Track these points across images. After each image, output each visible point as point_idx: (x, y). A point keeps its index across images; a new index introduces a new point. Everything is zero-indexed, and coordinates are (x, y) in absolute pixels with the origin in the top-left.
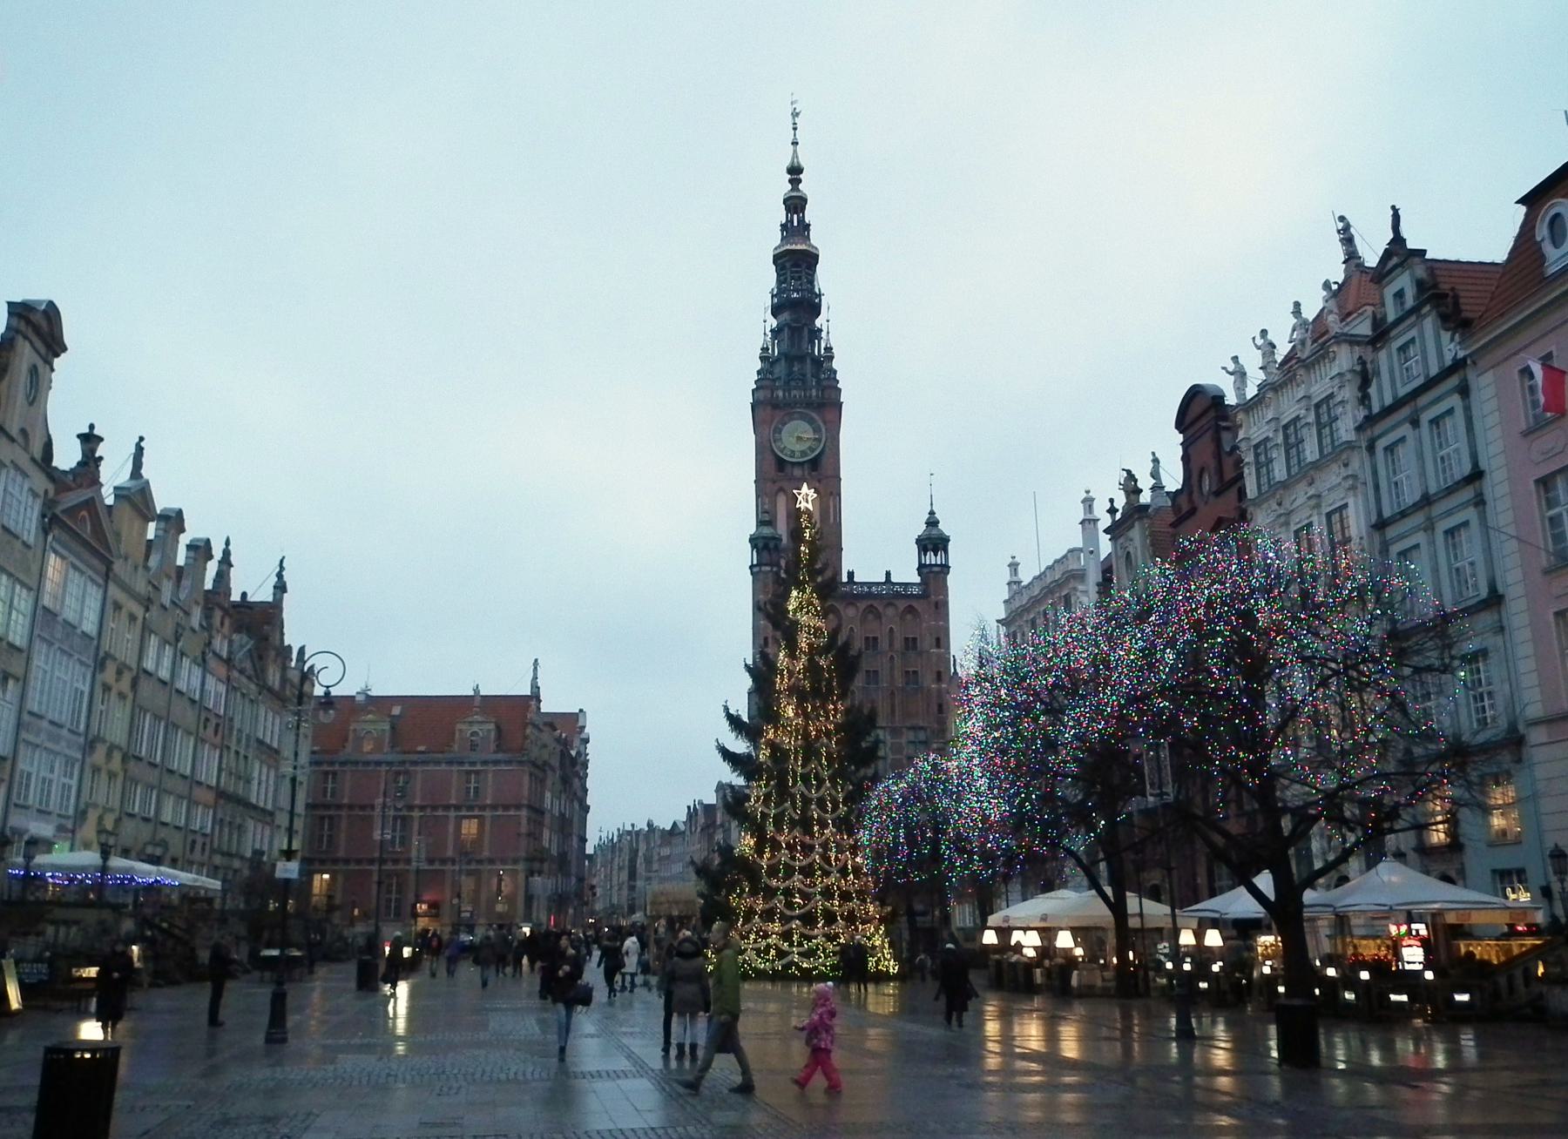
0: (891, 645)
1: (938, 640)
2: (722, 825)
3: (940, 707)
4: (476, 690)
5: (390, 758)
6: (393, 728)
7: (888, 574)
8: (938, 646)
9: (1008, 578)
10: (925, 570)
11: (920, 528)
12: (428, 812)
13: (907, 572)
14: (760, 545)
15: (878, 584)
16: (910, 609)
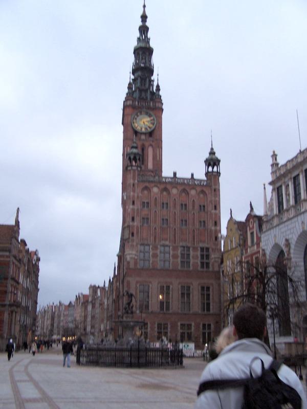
0: (193, 207)
2: (92, 302)
7: (192, 175)
9: (271, 162)
11: (207, 156)
13: (200, 175)
14: (132, 157)
15: (187, 179)
16: (203, 192)
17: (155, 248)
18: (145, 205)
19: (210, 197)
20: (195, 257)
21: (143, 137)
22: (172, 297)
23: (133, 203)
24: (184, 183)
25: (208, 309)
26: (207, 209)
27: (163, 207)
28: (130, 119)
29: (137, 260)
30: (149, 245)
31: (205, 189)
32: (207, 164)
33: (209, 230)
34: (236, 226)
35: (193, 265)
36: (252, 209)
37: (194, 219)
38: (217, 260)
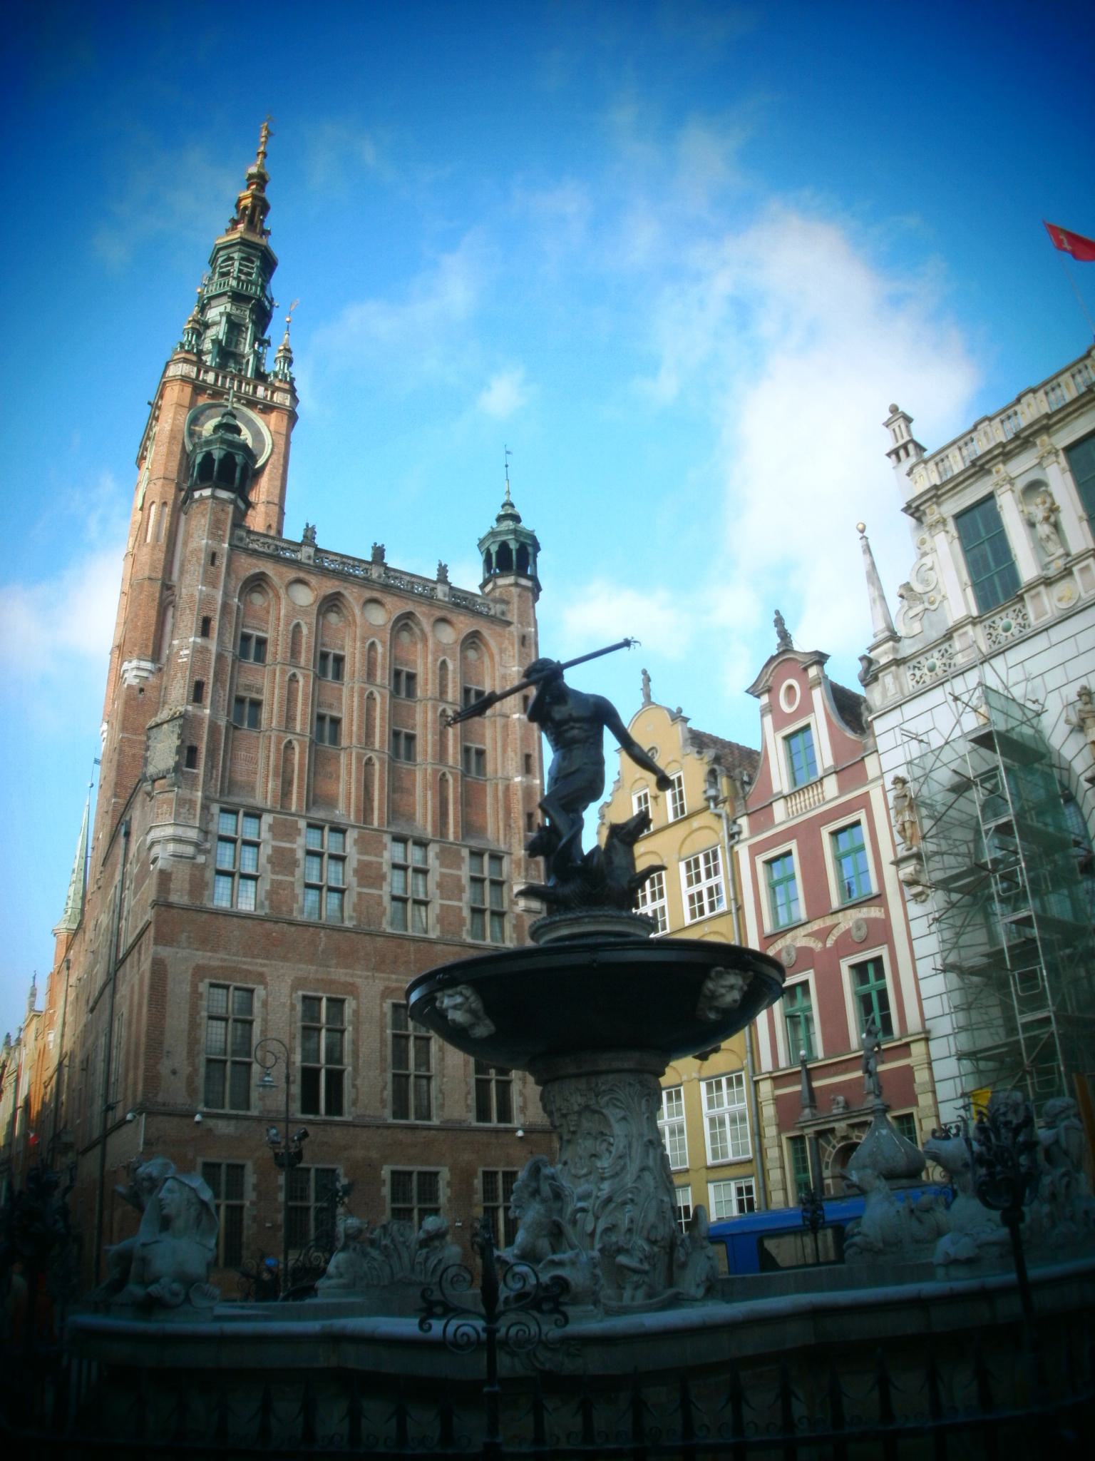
7: (443, 570)
14: (217, 454)
20: (450, 888)
22: (356, 1053)
25: (505, 1115)
27: (323, 672)
29: (204, 867)
30: (255, 814)
31: (486, 633)
32: (494, 549)
35: (441, 920)
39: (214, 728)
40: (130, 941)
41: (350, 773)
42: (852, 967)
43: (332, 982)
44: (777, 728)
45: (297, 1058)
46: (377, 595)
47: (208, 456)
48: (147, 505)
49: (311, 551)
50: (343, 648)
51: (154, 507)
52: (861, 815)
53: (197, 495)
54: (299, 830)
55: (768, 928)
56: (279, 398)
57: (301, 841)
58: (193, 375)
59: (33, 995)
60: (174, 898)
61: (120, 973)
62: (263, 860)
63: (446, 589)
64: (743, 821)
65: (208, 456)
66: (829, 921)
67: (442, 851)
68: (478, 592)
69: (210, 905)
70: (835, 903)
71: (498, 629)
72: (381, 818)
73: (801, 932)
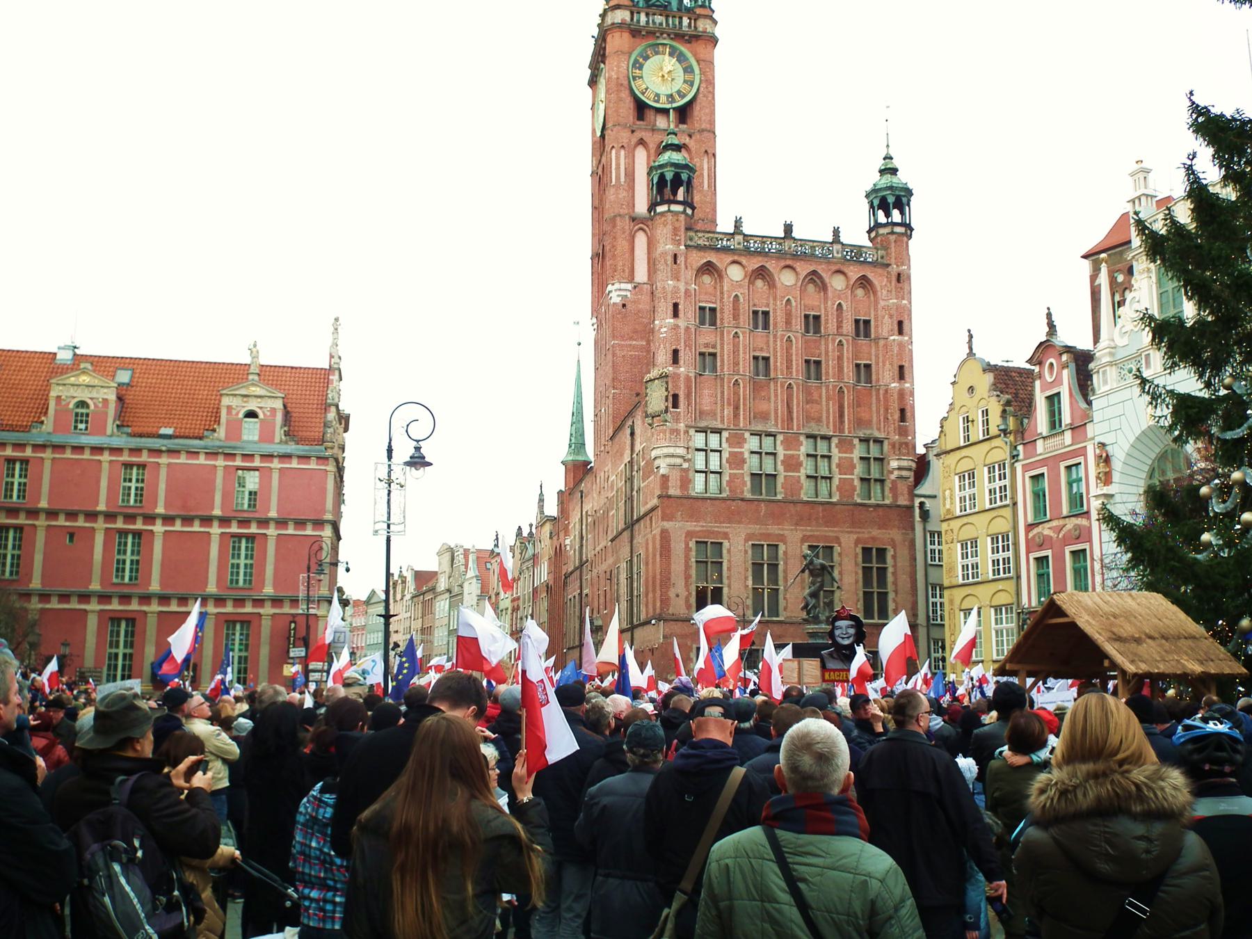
0: (839, 327)
1: (900, 323)
2: (449, 591)
3: (902, 411)
4: (253, 350)
5: (117, 442)
6: (120, 399)
7: (836, 232)
8: (901, 332)
10: (882, 231)
12: (178, 526)
13: (856, 234)
14: (669, 176)
16: (864, 282)
17: (737, 440)
18: (708, 316)
19: (886, 299)
20: (847, 467)
21: (661, 122)
23: (676, 314)
24: (813, 255)
26: (876, 332)
27: (756, 327)
28: (624, 65)
29: (687, 470)
30: (718, 431)
31: (870, 276)
32: (876, 202)
33: (881, 392)
34: (989, 378)
35: (839, 488)
36: (1052, 327)
37: (840, 358)
38: (904, 473)
39: (688, 379)
40: (643, 510)
41: (776, 395)
42: (1073, 553)
43: (769, 535)
44: (1042, 391)
45: (750, 583)
46: (789, 262)
47: (662, 177)
48: (608, 148)
49: (740, 238)
50: (768, 305)
51: (614, 151)
52: (1081, 459)
53: (660, 209)
54: (745, 440)
55: (1030, 520)
56: (702, 25)
57: (746, 446)
58: (628, 19)
59: (541, 500)
60: (672, 492)
61: (636, 527)
62: (724, 461)
63: (839, 247)
64: (1020, 448)
65: (662, 177)
66: (1061, 522)
67: (840, 441)
68: (864, 241)
69: (693, 494)
70: (1065, 512)
71: (880, 271)
72: (798, 425)
73: (1047, 525)
